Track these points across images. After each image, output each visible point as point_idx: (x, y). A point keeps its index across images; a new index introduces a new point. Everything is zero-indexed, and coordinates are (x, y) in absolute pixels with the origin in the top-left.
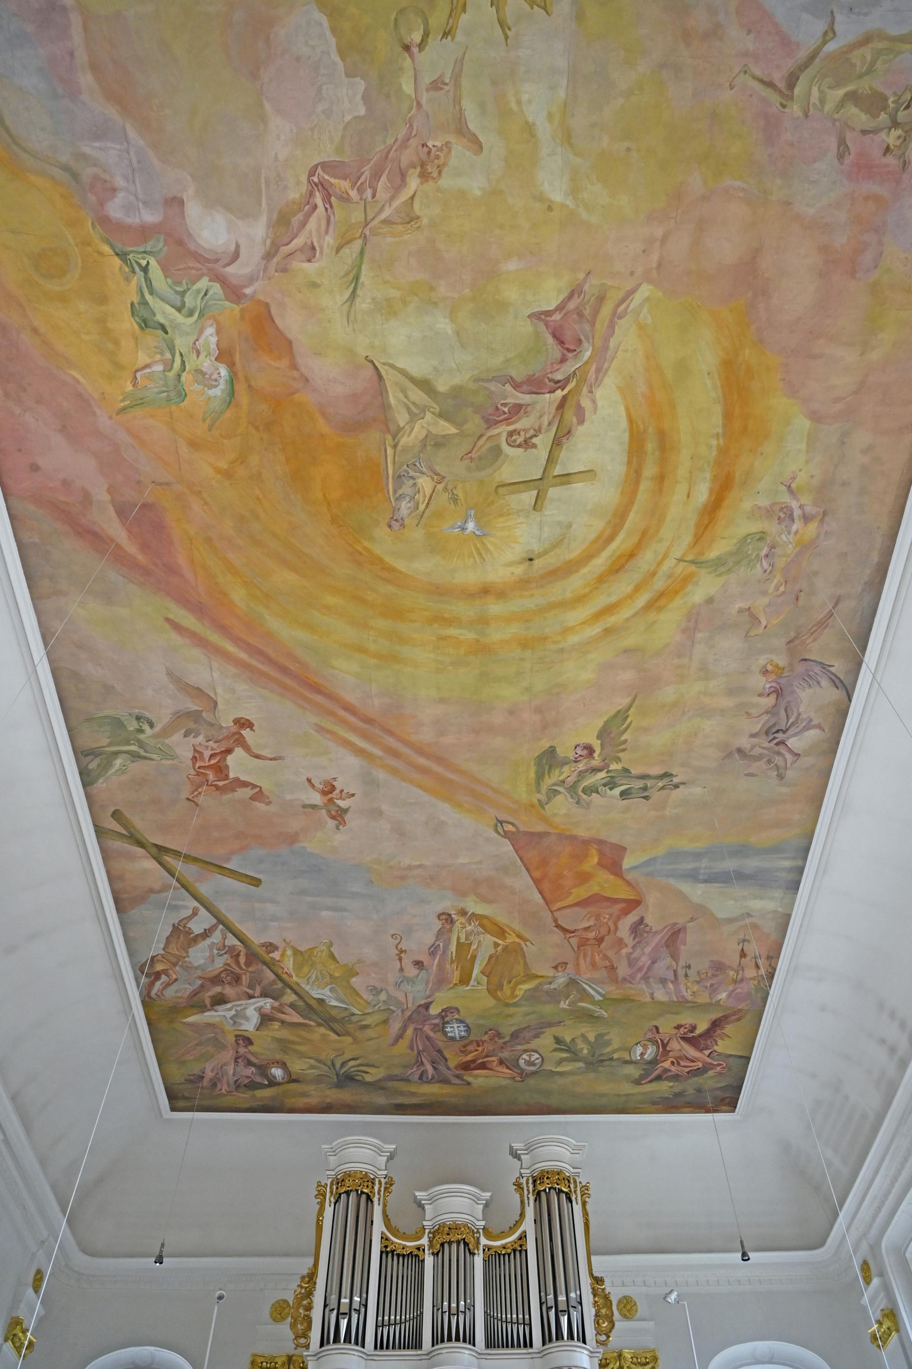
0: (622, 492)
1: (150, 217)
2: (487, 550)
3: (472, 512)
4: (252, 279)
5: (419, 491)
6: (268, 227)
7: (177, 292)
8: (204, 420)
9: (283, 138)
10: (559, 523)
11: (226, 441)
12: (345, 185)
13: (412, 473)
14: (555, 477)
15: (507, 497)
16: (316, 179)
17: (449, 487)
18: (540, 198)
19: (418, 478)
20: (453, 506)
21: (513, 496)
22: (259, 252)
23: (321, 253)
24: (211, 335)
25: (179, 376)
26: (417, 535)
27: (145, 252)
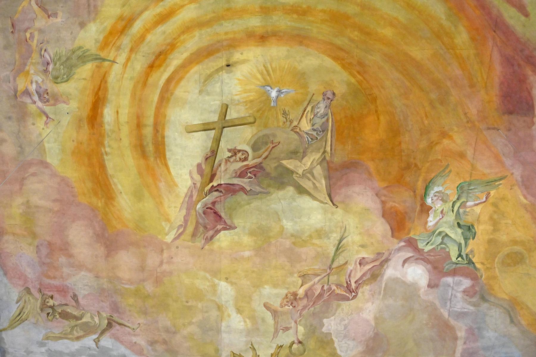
0: (165, 116)
1: (449, 280)
2: (262, 74)
3: (272, 105)
4: (399, 249)
5: (310, 120)
6: (384, 274)
7: (445, 244)
8: (450, 171)
9: (368, 311)
10: (208, 94)
11: (440, 158)
12: (338, 291)
13: (314, 133)
14: (214, 129)
15: (247, 115)
16: (353, 294)
17: (288, 123)
18: (232, 283)
19: (310, 130)
20: (287, 109)
21: (243, 115)
22: (391, 263)
23: (356, 261)
24: (431, 221)
25: (458, 199)
26: (314, 87)
27: (457, 264)
